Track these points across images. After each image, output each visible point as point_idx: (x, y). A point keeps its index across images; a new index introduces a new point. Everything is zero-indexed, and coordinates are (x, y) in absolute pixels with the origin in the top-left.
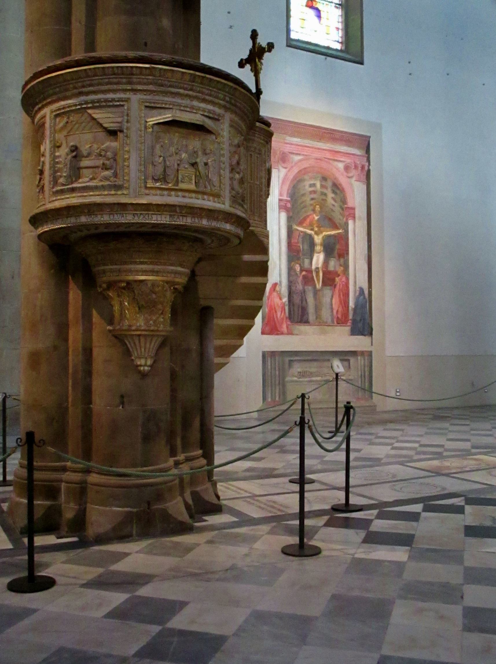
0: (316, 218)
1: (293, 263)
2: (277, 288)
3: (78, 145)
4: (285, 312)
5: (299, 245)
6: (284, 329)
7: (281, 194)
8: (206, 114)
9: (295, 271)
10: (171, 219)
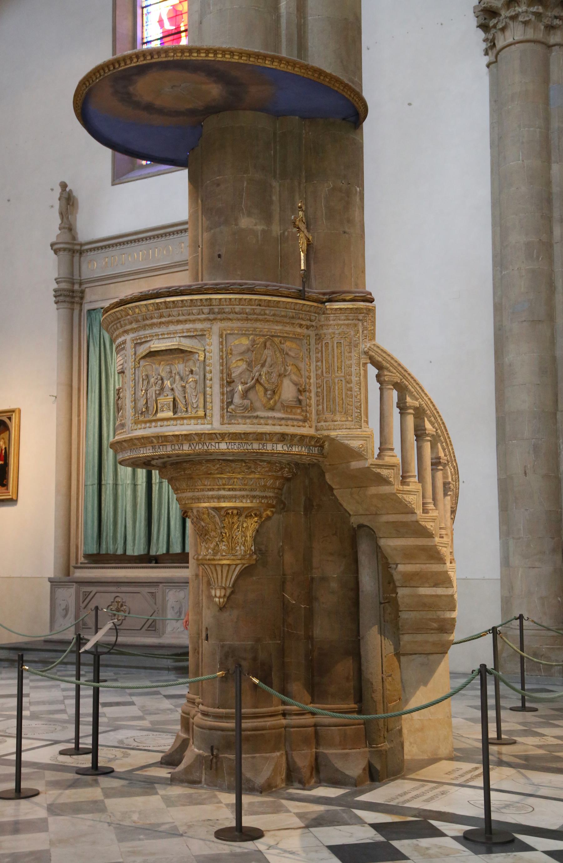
8: (185, 334)
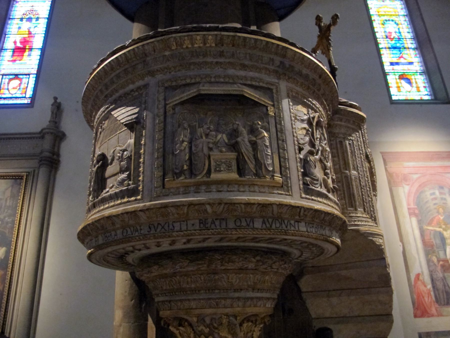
0: (442, 218)
1: (430, 256)
2: (421, 278)
3: (106, 153)
4: (431, 298)
5: (431, 241)
6: (433, 310)
7: (408, 204)
8: (249, 82)
9: (433, 262)
10: (202, 225)
